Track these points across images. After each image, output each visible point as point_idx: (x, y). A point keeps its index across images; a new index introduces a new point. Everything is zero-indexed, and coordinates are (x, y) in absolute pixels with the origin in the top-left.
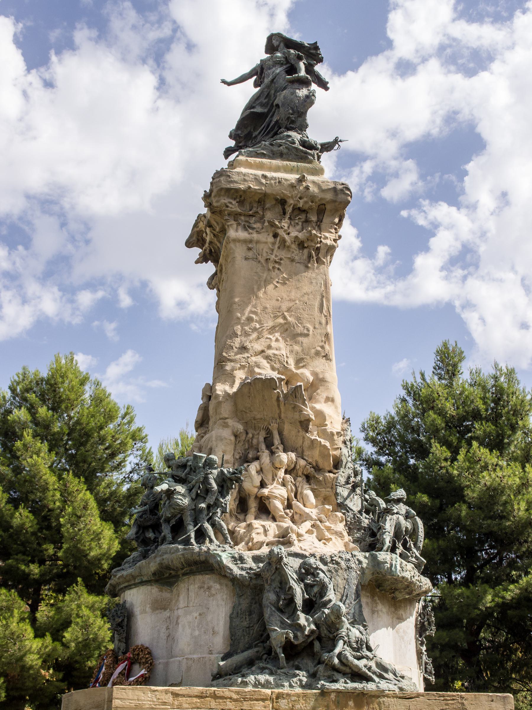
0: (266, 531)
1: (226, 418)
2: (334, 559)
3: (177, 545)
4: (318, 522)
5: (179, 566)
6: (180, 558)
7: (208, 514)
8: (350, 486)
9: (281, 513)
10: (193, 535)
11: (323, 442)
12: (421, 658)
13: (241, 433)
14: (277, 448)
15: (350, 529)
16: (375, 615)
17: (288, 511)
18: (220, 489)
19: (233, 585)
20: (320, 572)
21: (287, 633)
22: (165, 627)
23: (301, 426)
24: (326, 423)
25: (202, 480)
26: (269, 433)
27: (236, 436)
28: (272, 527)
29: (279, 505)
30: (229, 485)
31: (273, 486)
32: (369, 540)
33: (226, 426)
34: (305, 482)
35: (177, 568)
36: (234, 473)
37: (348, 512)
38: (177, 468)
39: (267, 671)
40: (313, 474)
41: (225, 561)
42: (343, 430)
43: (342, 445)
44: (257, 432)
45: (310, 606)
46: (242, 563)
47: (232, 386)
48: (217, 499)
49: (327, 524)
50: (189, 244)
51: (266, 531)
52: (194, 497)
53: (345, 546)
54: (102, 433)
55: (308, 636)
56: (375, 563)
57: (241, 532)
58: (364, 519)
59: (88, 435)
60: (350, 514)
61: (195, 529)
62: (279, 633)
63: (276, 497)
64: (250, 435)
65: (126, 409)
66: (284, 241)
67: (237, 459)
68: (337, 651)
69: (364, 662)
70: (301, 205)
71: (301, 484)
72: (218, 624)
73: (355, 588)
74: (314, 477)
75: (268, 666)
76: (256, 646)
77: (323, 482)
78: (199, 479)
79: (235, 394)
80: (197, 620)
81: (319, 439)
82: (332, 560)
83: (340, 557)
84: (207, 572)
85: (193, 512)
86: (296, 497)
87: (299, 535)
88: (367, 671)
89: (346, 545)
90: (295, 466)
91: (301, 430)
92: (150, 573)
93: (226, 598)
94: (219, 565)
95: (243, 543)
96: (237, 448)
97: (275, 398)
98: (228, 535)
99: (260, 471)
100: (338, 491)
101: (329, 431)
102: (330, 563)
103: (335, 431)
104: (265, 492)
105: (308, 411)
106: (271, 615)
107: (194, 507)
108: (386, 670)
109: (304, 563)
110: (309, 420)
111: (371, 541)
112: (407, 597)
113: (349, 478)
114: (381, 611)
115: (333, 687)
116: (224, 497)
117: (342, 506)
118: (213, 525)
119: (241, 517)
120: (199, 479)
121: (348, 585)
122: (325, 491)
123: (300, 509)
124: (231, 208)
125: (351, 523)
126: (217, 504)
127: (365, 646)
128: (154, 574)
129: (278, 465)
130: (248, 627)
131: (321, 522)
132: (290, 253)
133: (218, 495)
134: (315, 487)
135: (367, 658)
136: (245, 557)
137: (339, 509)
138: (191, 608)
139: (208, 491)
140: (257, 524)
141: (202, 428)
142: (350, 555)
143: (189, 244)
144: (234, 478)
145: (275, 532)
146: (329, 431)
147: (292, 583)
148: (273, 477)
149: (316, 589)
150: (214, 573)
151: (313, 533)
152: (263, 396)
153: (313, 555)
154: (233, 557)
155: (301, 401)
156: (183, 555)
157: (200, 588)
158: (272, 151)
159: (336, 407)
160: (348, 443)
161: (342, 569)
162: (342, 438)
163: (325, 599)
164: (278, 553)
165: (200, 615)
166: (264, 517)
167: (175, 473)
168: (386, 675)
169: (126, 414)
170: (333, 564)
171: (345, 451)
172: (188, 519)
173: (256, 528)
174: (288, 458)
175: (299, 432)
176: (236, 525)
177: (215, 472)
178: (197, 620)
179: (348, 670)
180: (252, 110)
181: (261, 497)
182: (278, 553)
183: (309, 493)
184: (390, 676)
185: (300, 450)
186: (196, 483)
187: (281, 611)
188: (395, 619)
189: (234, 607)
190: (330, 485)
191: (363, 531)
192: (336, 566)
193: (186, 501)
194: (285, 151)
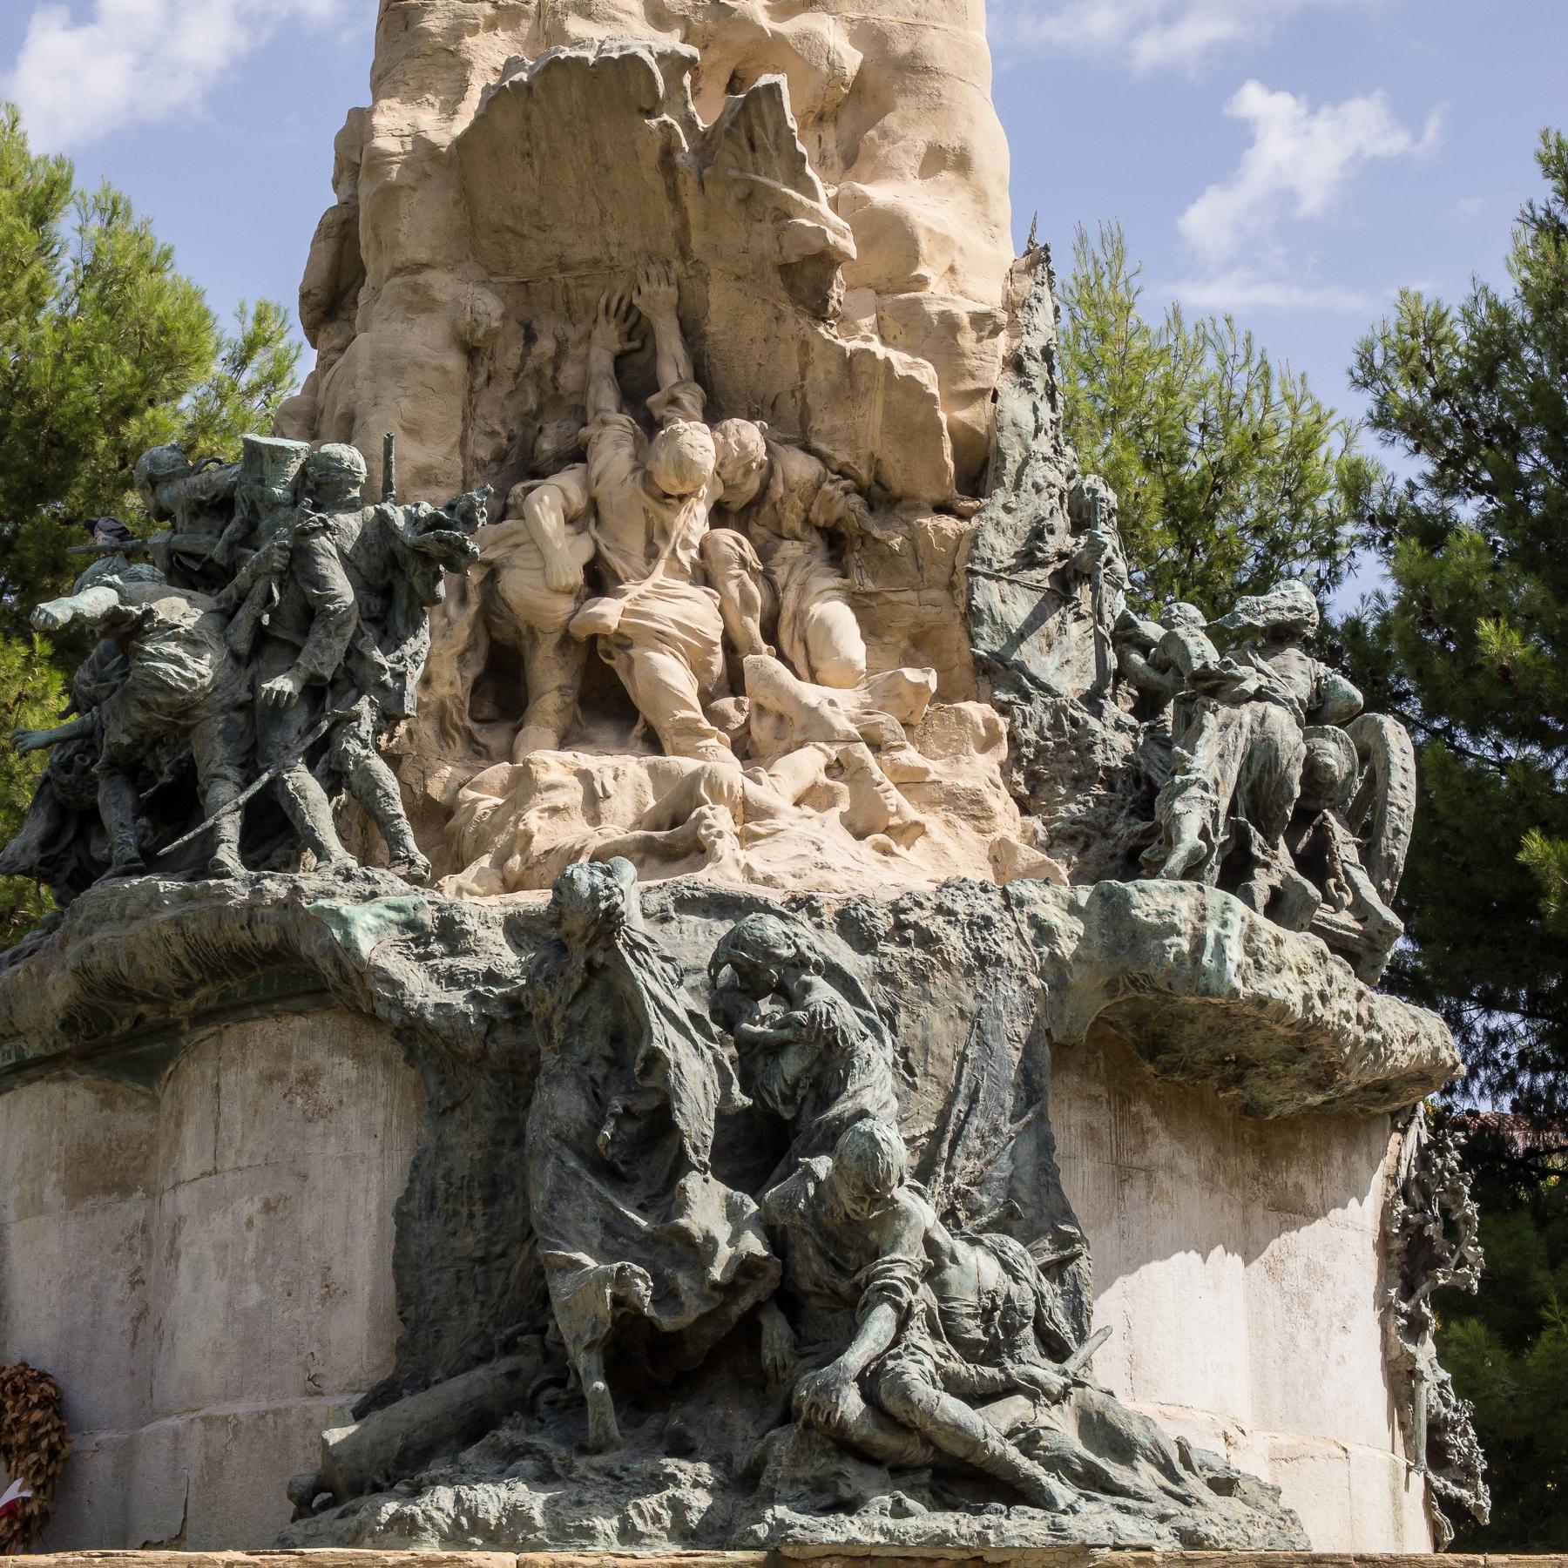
0: (593, 801)
1: (422, 267)
2: (911, 917)
3: (153, 878)
4: (863, 751)
5: (166, 975)
6: (167, 940)
7: (313, 726)
8: (1041, 575)
9: (684, 714)
10: (230, 828)
11: (901, 361)
12: (1412, 1398)
13: (492, 334)
14: (674, 401)
15: (1033, 778)
16: (1136, 1191)
17: (727, 703)
18: (376, 604)
19: (410, 1059)
20: (817, 980)
21: (621, 1278)
22: (123, 1276)
23: (791, 288)
24: (922, 270)
25: (278, 562)
26: (637, 329)
27: (471, 352)
28: (627, 778)
29: (676, 674)
30: (417, 583)
31: (648, 585)
32: (1126, 828)
33: (422, 303)
34: (817, 562)
35: (158, 986)
36: (435, 523)
37: (1027, 698)
38: (194, 516)
39: (527, 1464)
40: (861, 519)
41: (366, 946)
42: (1011, 306)
43: (996, 376)
44: (582, 328)
45: (758, 1146)
46: (453, 952)
47: (450, 110)
48: (353, 652)
49: (910, 756)
51: (593, 801)
52: (243, 647)
53: (994, 860)
54: (133, 429)
55: (729, 1289)
56: (1116, 927)
57: (482, 807)
58: (1109, 734)
59: (64, 448)
60: (1038, 709)
61: (242, 799)
62: (589, 1275)
63: (662, 637)
64: (546, 346)
65: (250, 325)
67: (480, 464)
68: (857, 1356)
69: (1016, 1409)
71: (798, 575)
72: (346, 1251)
73: (1016, 1056)
74: (865, 536)
75: (537, 1440)
76: (509, 1347)
77: (908, 563)
78: (268, 556)
79: (461, 143)
80: (252, 1236)
81: (881, 351)
82: (900, 926)
83: (940, 909)
84: (300, 1003)
85: (240, 717)
86: (770, 632)
87: (749, 812)
88: (1014, 1454)
89: (1000, 855)
90: (765, 487)
91: (788, 309)
92: (51, 1022)
93: (387, 1124)
94: (338, 963)
95: (485, 861)
96: (484, 408)
97: (652, 156)
98: (404, 825)
99: (587, 516)
100: (979, 600)
101: (933, 308)
102: (888, 938)
103: (962, 310)
104: (610, 611)
105: (823, 212)
107: (243, 695)
108: (1122, 1447)
109: (734, 941)
110: (827, 259)
111: (1119, 829)
112: (1317, 1099)
113: (1038, 533)
114: (1171, 1168)
115: (829, 1536)
116: (391, 640)
117: (999, 674)
118: (334, 781)
119: (493, 738)
120: (268, 556)
121: (982, 1042)
122: (914, 604)
123: (780, 689)
125: (1040, 751)
126: (353, 676)
127: (1028, 1332)
128: (68, 1024)
129: (668, 482)
130: (482, 1260)
131: (876, 747)
133: (359, 634)
134: (870, 586)
135: (1034, 1390)
136: (471, 924)
137: (985, 686)
138: (230, 1177)
139: (311, 612)
140: (554, 765)
141: (332, 329)
142: (997, 900)
144: (434, 549)
145: (641, 803)
146: (933, 308)
147: (663, 1034)
148: (650, 542)
149: (792, 1065)
150: (329, 1006)
151: (832, 803)
152: (596, 149)
153: (805, 904)
154: (410, 925)
156: (177, 922)
157: (269, 1079)
159: (980, 197)
160: (1035, 368)
161: (947, 965)
162: (1002, 344)
163: (835, 1110)
164: (594, 889)
165: (268, 1208)
166: (606, 733)
167: (183, 541)
168: (1117, 1472)
169: (251, 345)
170: (905, 942)
171: (1017, 406)
172: (214, 751)
173: (552, 787)
174: (722, 448)
175: (779, 318)
176: (463, 775)
177: (350, 523)
178: (252, 1236)
179: (915, 1452)
181: (593, 639)
182: (594, 889)
183: (838, 617)
184: (1145, 1477)
185: (789, 407)
186: (255, 577)
187: (610, 1172)
188: (1258, 1210)
189: (415, 1166)
190: (939, 574)
191: (1099, 790)
192: (918, 954)
193: (203, 668)
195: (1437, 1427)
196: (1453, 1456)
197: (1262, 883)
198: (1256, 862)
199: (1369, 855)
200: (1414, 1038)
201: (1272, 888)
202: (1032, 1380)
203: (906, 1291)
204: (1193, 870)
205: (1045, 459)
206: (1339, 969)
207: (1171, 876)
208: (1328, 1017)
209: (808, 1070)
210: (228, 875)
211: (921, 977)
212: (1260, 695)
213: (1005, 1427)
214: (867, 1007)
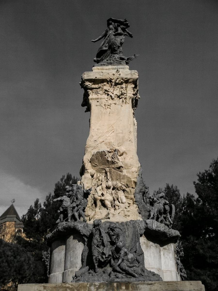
28: (104, 212)
39: (91, 274)
50: (83, 105)
52: (71, 202)
55: (108, 257)
66: (111, 96)
70: (117, 82)
77: (130, 193)
81: (126, 174)
87: (114, 215)
106: (94, 249)
108: (144, 271)
124: (89, 86)
131: (126, 208)
132: (114, 101)
135: (136, 266)
136: (89, 225)
143: (83, 105)
153: (117, 222)
155: (117, 159)
158: (108, 63)
160: (140, 175)
161: (130, 228)
180: (101, 49)
194: (112, 62)
195: (180, 269)
196: (183, 271)
197: (160, 220)
198: (159, 218)
199: (171, 217)
200: (175, 233)
201: (161, 220)
202: (136, 265)
203: (123, 257)
204: (153, 218)
205: (141, 183)
206: (166, 227)
207: (150, 219)
208: (165, 231)
209: (116, 237)
210: (69, 222)
211: (128, 229)
212: (159, 203)
213: (132, 270)
214: (122, 231)
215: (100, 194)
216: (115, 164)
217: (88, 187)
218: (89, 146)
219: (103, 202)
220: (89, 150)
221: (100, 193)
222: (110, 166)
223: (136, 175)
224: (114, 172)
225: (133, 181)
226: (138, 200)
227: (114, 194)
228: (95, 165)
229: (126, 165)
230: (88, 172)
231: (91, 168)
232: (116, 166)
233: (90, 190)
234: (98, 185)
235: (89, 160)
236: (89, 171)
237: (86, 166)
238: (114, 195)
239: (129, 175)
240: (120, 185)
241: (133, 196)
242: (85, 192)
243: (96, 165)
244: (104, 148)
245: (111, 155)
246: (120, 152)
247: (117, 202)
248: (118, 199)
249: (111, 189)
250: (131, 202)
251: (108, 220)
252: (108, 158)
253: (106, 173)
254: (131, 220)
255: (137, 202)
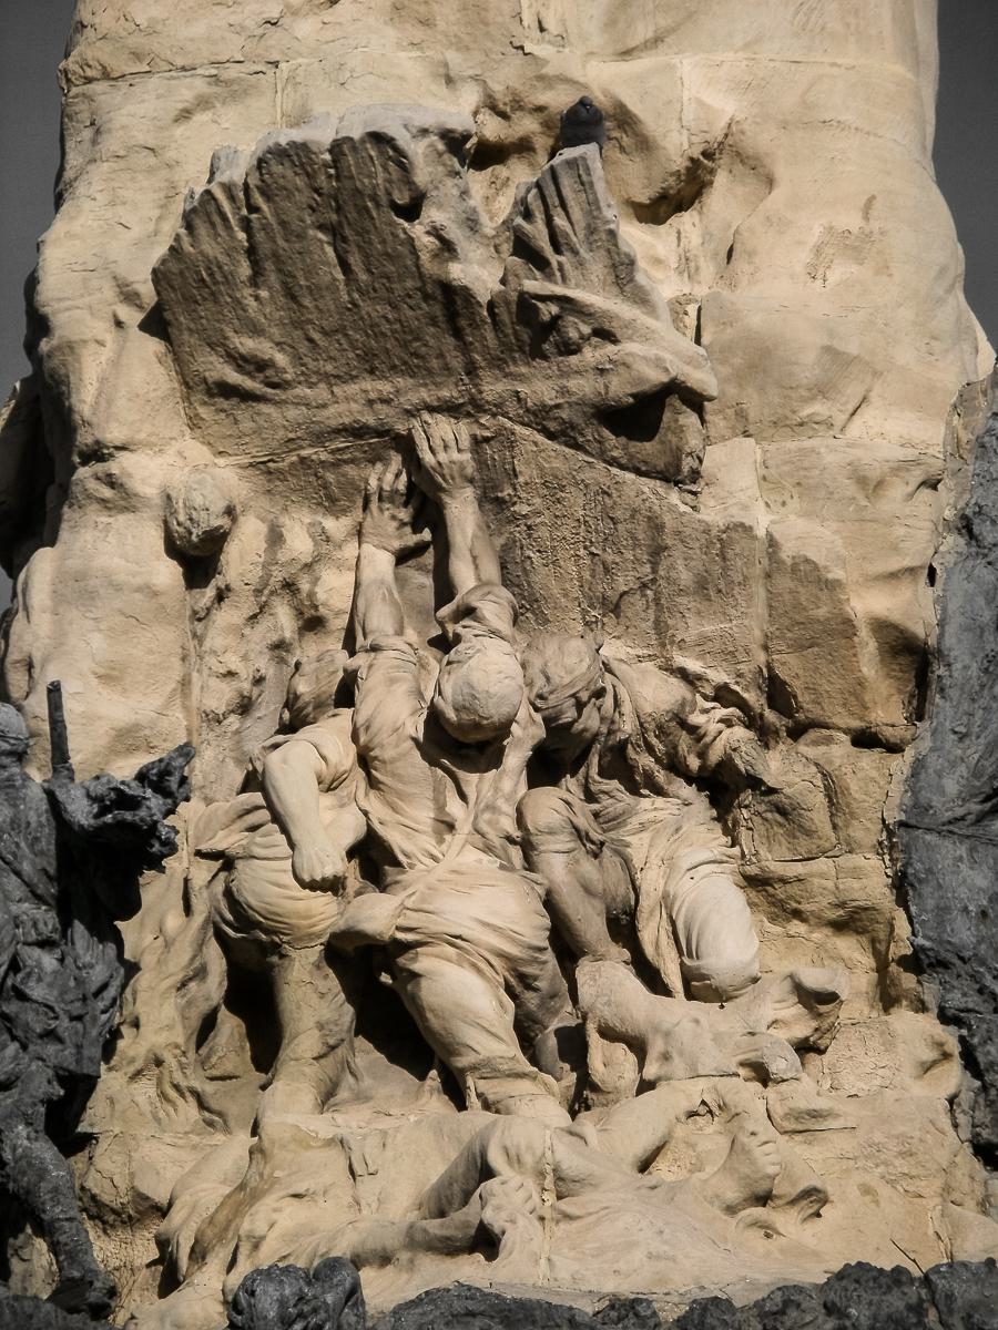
77: (819, 817)
87: (564, 1185)
131: (762, 1074)
155: (597, 267)
215: (329, 858)
216: (569, 348)
217: (127, 738)
218: (137, 56)
219: (379, 984)
220: (133, 112)
221: (327, 835)
222: (493, 387)
223: (918, 525)
224: (553, 487)
225: (881, 627)
226: (964, 933)
227: (564, 841)
228: (233, 377)
229: (760, 361)
230: (122, 498)
231: (171, 421)
232: (584, 387)
233: (166, 780)
234: (291, 702)
235: (130, 297)
236: (145, 471)
237: (85, 398)
238: (558, 864)
239: (805, 533)
240: (653, 692)
241: (870, 880)
242: (81, 812)
243: (257, 366)
244: (380, 82)
245: (495, 196)
246: (645, 145)
247: (608, 982)
248: (624, 927)
249: (516, 757)
250: (847, 969)
251: (471, 1270)
252: (447, 248)
253: (424, 502)
254: (856, 1275)
255: (944, 965)
